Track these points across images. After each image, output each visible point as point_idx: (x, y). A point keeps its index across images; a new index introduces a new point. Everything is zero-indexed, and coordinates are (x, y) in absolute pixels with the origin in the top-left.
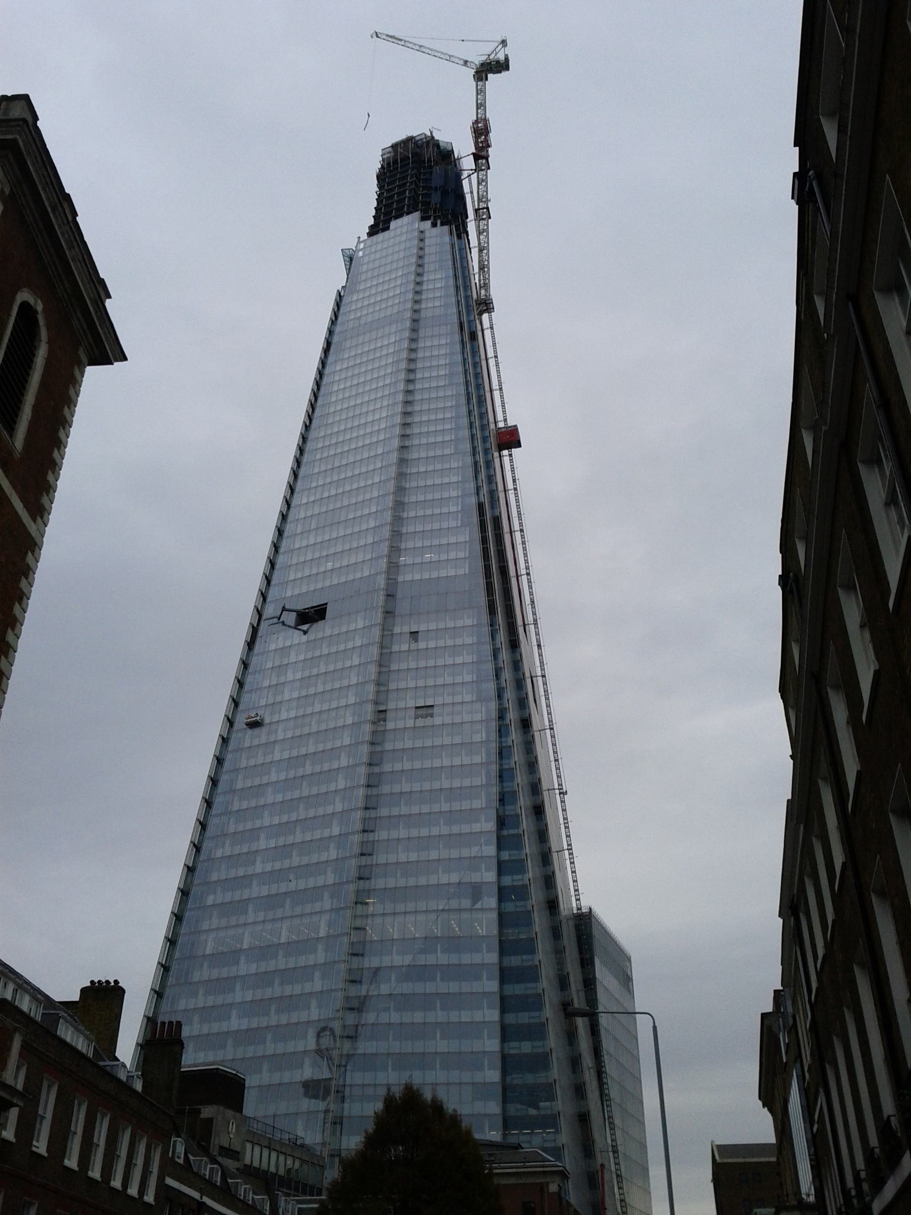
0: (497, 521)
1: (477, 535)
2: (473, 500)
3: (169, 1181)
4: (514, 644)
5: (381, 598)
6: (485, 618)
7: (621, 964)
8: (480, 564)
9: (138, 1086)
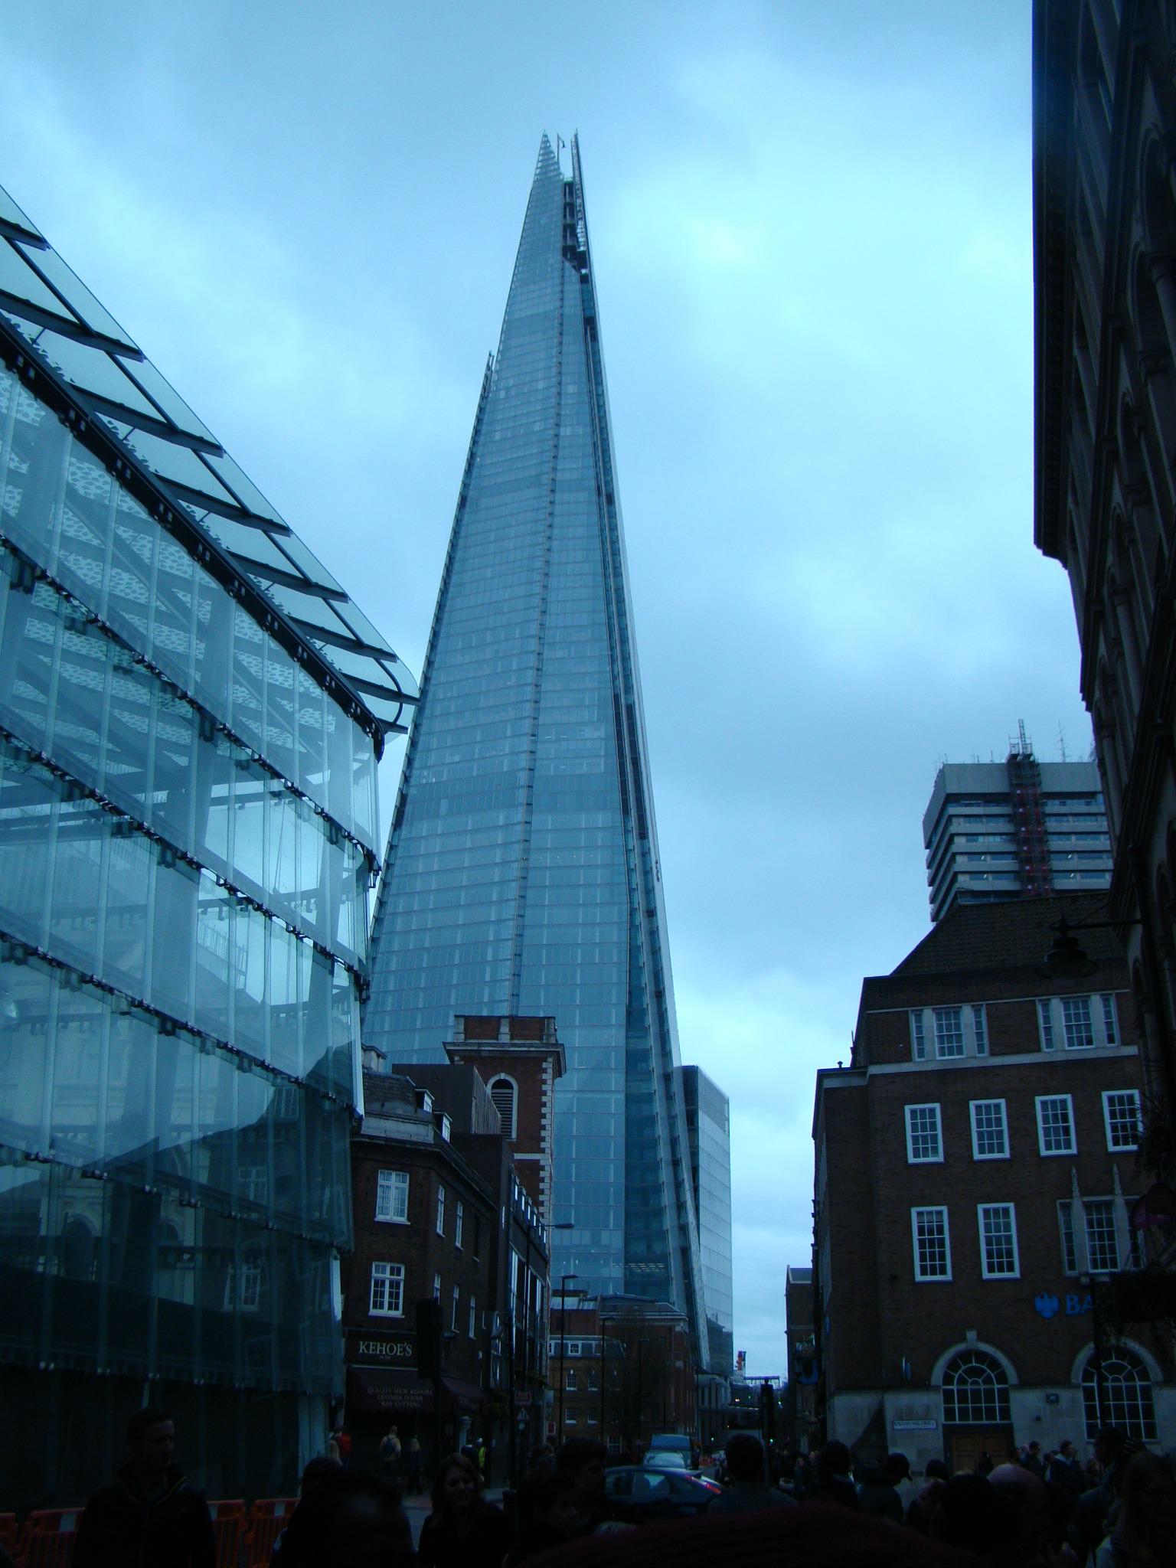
0: (630, 709)
2: (610, 693)
4: (643, 834)
5: (522, 795)
6: (619, 816)
7: (721, 1102)
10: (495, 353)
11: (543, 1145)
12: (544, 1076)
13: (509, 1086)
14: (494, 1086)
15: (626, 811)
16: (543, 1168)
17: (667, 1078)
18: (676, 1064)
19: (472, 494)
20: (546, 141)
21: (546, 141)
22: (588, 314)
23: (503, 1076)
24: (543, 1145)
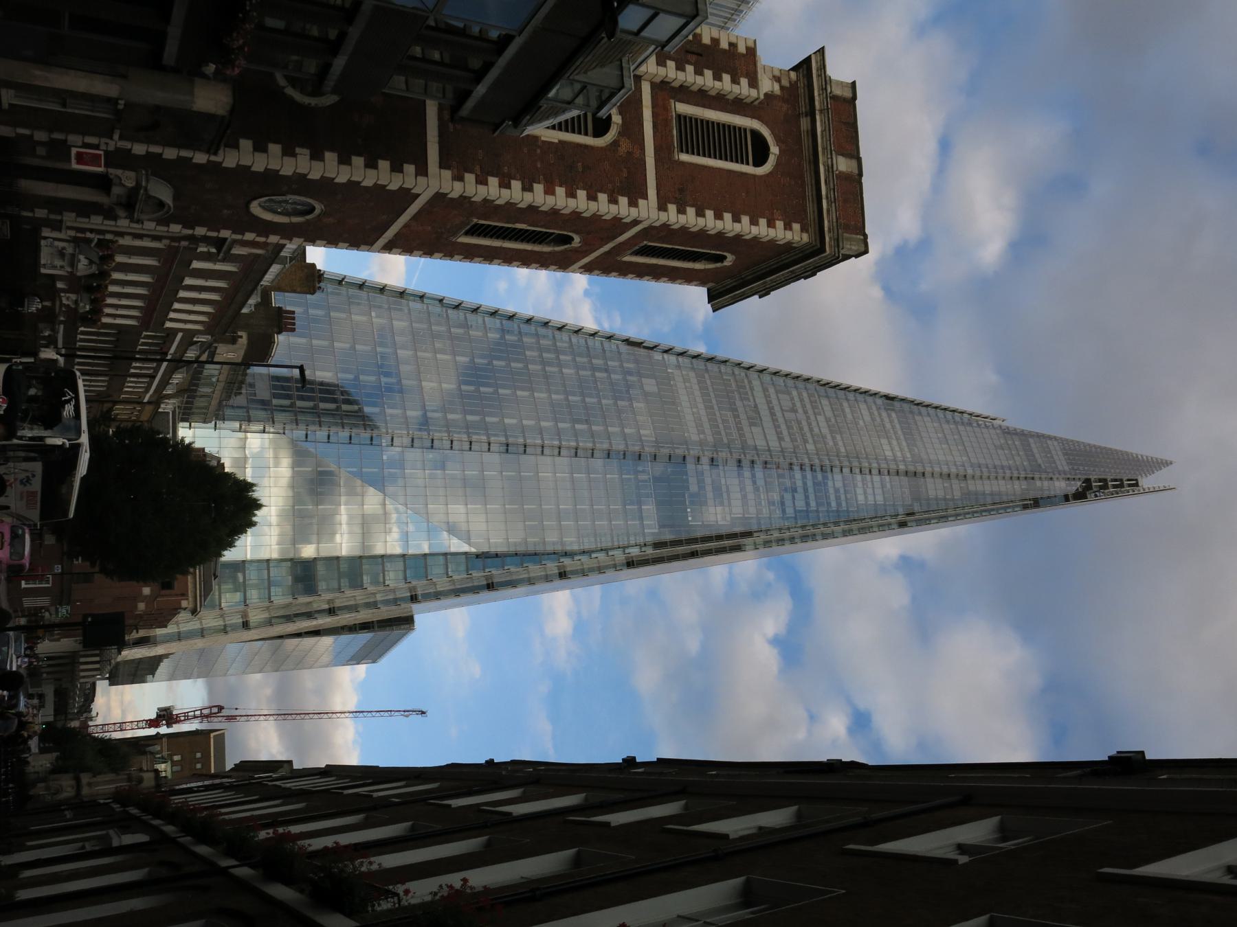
0: (738, 548)
1: (723, 531)
2: (755, 528)
3: (180, 335)
4: (631, 564)
8: (699, 534)
9: (245, 311)
10: (1005, 424)
11: (672, 208)
12: (780, 224)
13: (760, 160)
14: (756, 135)
15: (657, 545)
16: (633, 203)
17: (414, 599)
18: (415, 607)
19: (897, 404)
20: (1167, 463)
21: (1167, 463)
22: (1041, 502)
23: (774, 149)
24: (672, 208)
